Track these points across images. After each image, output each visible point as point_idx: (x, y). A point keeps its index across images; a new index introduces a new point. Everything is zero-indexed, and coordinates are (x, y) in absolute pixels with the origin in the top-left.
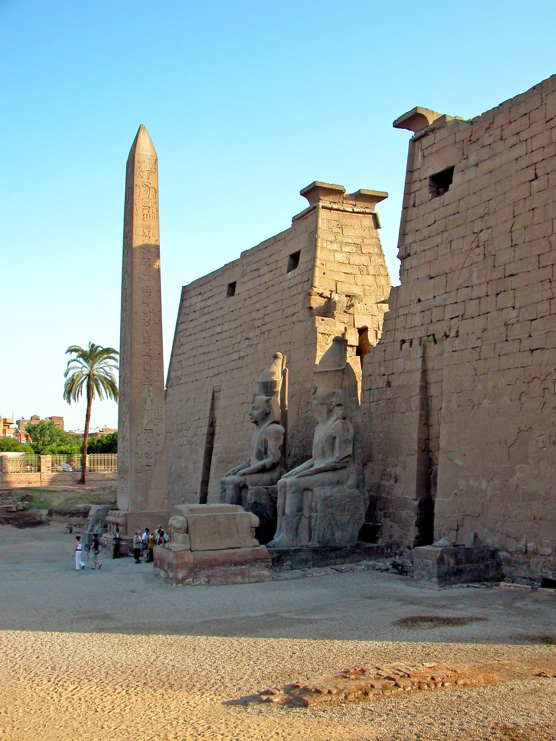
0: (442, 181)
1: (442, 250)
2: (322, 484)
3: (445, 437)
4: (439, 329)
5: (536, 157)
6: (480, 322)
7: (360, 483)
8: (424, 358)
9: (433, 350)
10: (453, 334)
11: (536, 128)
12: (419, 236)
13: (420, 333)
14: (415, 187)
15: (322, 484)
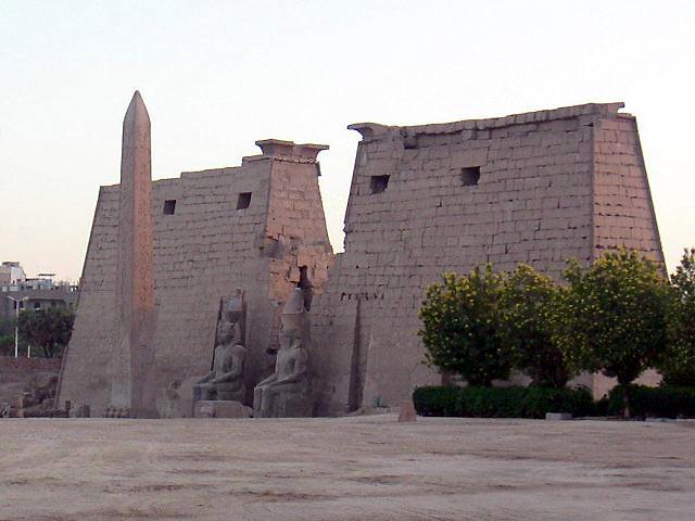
0: (380, 182)
1: (378, 235)
2: (286, 391)
3: (370, 363)
4: (371, 291)
5: (443, 192)
6: (398, 293)
7: (309, 392)
8: (358, 308)
9: (365, 304)
10: (379, 296)
11: (444, 172)
12: (359, 219)
13: (358, 291)
14: (360, 180)
15: (286, 391)
